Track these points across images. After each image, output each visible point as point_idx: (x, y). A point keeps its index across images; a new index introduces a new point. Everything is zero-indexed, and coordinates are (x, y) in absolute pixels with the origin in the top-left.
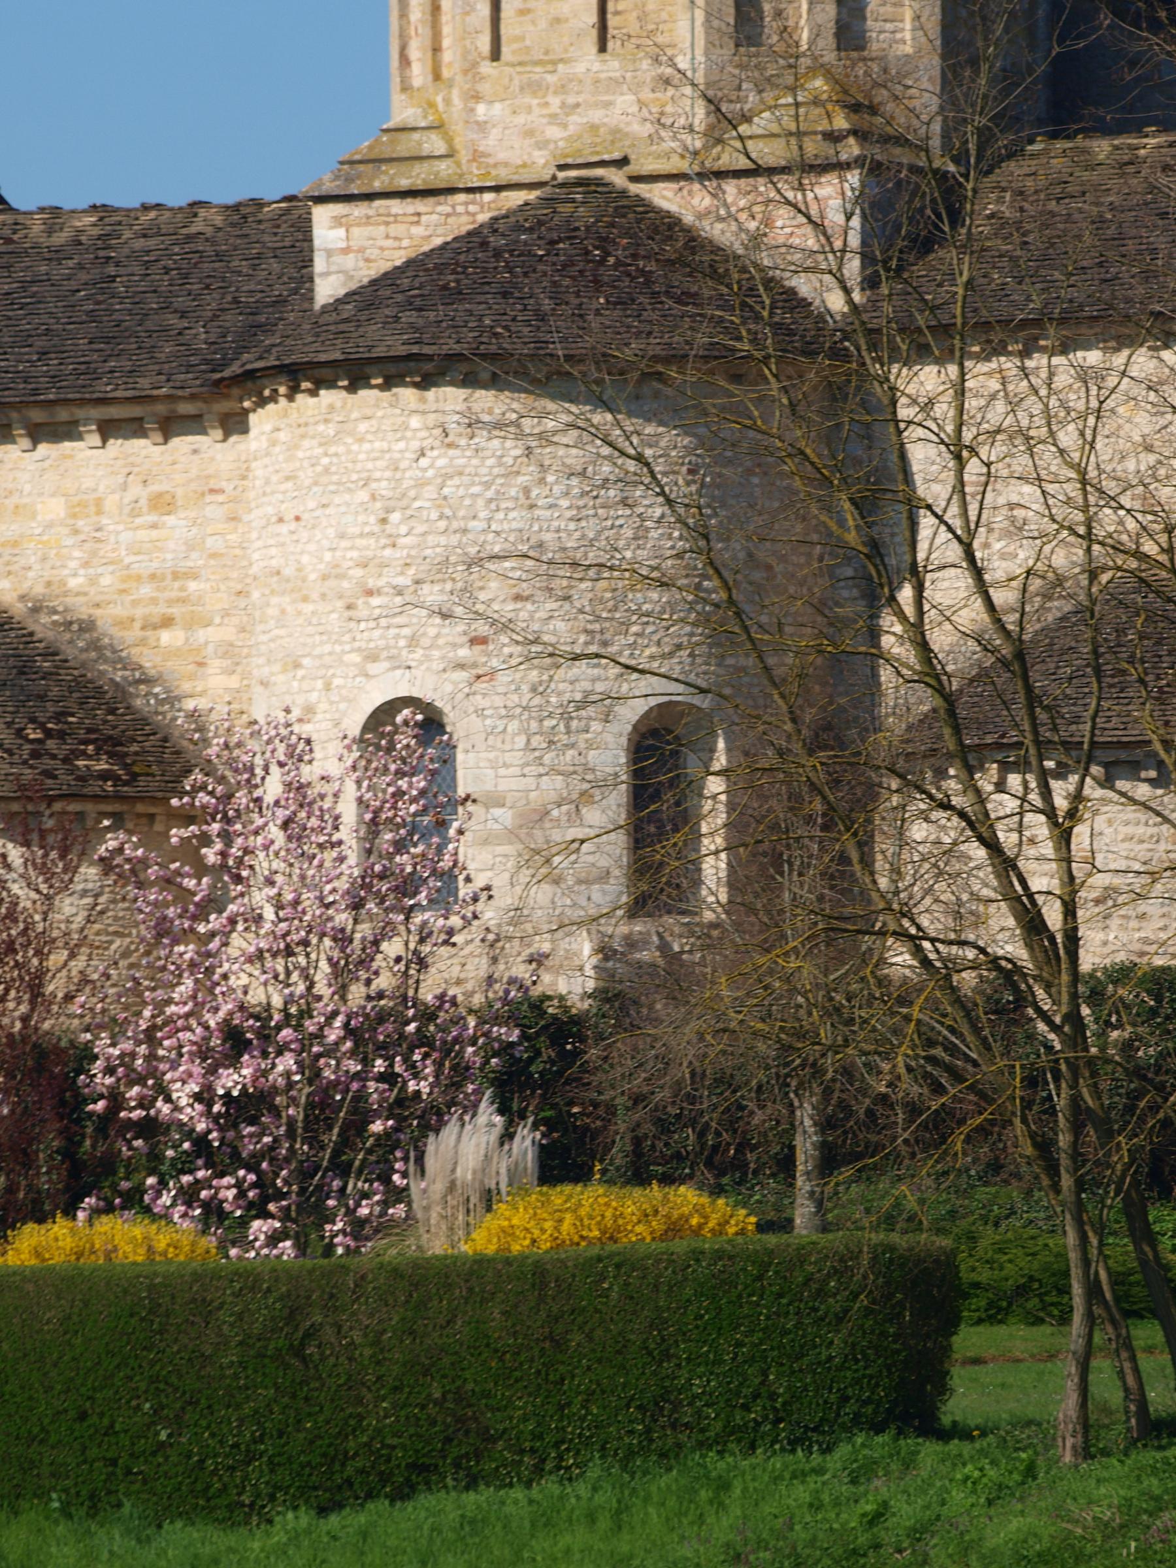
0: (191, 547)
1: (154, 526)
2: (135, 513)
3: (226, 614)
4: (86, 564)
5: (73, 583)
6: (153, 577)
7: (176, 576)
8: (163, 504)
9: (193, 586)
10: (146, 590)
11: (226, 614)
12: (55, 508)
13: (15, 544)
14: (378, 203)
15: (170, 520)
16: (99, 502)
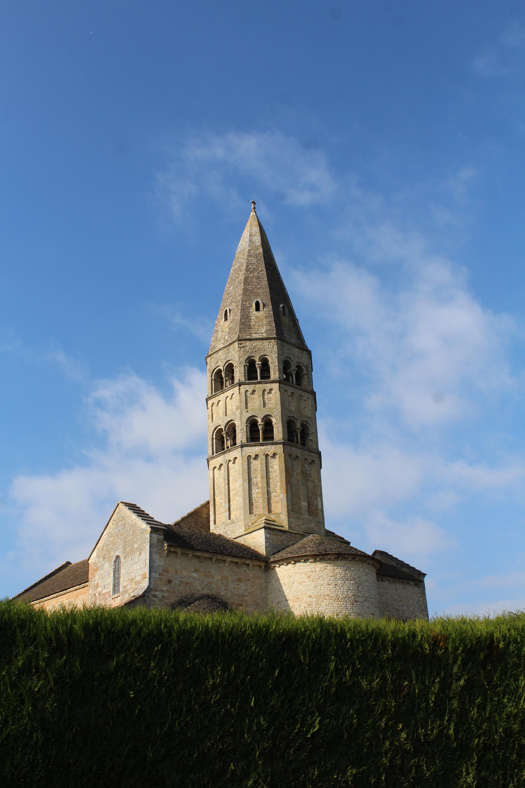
0: (245, 590)
1: (238, 585)
2: (234, 581)
3: (252, 605)
4: (225, 590)
5: (222, 593)
6: (238, 595)
7: (242, 596)
8: (239, 580)
9: (246, 598)
10: (237, 597)
11: (252, 605)
12: (219, 577)
13: (211, 583)
14: (275, 531)
15: (241, 584)
16: (227, 578)
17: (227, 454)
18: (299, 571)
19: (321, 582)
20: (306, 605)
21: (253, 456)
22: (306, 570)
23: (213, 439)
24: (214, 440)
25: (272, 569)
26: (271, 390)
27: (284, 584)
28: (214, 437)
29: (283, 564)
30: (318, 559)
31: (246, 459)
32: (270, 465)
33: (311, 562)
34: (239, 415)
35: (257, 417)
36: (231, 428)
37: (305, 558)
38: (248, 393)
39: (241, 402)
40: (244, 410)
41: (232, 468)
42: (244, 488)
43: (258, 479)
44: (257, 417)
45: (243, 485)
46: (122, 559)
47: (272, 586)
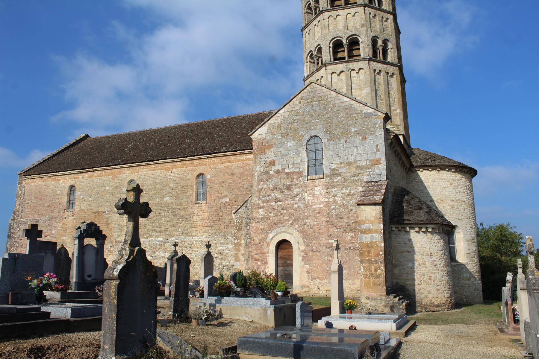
17: (351, 63)
18: (442, 177)
19: (458, 189)
20: (450, 207)
21: (377, 71)
22: (448, 178)
23: (330, 47)
24: (331, 49)
25: (413, 172)
26: (387, 19)
27: (428, 186)
28: (331, 45)
29: (428, 170)
30: (458, 170)
31: (372, 71)
32: (390, 82)
33: (453, 172)
34: (365, 32)
35: (378, 38)
36: (354, 43)
37: (450, 168)
38: (371, 16)
39: (366, 21)
40: (369, 30)
41: (355, 77)
42: (372, 97)
43: (382, 91)
44: (378, 38)
45: (372, 94)
46: (325, 140)
47: (413, 186)
